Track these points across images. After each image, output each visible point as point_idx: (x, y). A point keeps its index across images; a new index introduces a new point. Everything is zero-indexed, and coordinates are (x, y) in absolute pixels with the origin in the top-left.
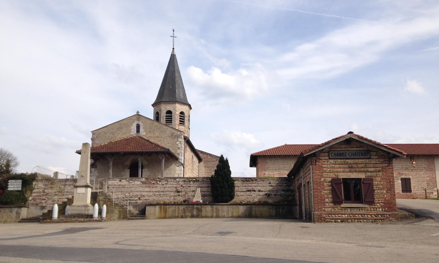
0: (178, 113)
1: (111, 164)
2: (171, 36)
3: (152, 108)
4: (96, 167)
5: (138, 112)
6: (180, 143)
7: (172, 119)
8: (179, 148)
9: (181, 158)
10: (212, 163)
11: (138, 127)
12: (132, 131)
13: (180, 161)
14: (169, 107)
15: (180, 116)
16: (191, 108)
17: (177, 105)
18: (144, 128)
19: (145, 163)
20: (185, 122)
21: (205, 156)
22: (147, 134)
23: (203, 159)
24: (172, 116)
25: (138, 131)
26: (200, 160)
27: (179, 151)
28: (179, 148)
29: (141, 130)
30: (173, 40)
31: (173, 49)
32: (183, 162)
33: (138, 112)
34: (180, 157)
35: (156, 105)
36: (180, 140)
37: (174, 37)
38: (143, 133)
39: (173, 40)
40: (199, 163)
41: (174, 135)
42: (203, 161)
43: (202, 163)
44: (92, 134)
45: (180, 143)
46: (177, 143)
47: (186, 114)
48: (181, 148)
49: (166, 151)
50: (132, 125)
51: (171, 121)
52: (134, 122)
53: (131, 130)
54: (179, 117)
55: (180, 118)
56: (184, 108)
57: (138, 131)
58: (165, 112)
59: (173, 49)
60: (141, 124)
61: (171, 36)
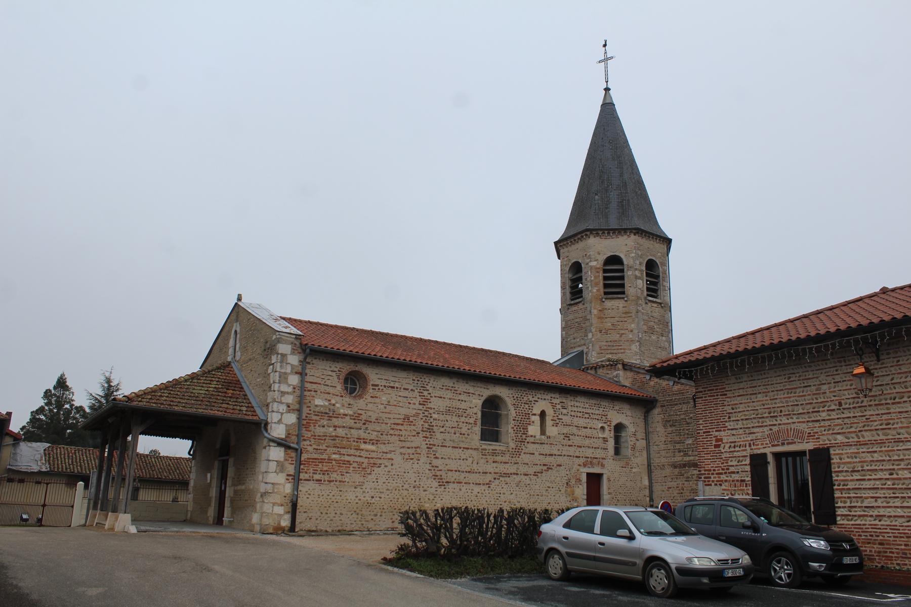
15: (605, 271)
16: (669, 241)
17: (592, 241)
42: (658, 404)
43: (656, 411)
54: (601, 275)
55: (605, 278)
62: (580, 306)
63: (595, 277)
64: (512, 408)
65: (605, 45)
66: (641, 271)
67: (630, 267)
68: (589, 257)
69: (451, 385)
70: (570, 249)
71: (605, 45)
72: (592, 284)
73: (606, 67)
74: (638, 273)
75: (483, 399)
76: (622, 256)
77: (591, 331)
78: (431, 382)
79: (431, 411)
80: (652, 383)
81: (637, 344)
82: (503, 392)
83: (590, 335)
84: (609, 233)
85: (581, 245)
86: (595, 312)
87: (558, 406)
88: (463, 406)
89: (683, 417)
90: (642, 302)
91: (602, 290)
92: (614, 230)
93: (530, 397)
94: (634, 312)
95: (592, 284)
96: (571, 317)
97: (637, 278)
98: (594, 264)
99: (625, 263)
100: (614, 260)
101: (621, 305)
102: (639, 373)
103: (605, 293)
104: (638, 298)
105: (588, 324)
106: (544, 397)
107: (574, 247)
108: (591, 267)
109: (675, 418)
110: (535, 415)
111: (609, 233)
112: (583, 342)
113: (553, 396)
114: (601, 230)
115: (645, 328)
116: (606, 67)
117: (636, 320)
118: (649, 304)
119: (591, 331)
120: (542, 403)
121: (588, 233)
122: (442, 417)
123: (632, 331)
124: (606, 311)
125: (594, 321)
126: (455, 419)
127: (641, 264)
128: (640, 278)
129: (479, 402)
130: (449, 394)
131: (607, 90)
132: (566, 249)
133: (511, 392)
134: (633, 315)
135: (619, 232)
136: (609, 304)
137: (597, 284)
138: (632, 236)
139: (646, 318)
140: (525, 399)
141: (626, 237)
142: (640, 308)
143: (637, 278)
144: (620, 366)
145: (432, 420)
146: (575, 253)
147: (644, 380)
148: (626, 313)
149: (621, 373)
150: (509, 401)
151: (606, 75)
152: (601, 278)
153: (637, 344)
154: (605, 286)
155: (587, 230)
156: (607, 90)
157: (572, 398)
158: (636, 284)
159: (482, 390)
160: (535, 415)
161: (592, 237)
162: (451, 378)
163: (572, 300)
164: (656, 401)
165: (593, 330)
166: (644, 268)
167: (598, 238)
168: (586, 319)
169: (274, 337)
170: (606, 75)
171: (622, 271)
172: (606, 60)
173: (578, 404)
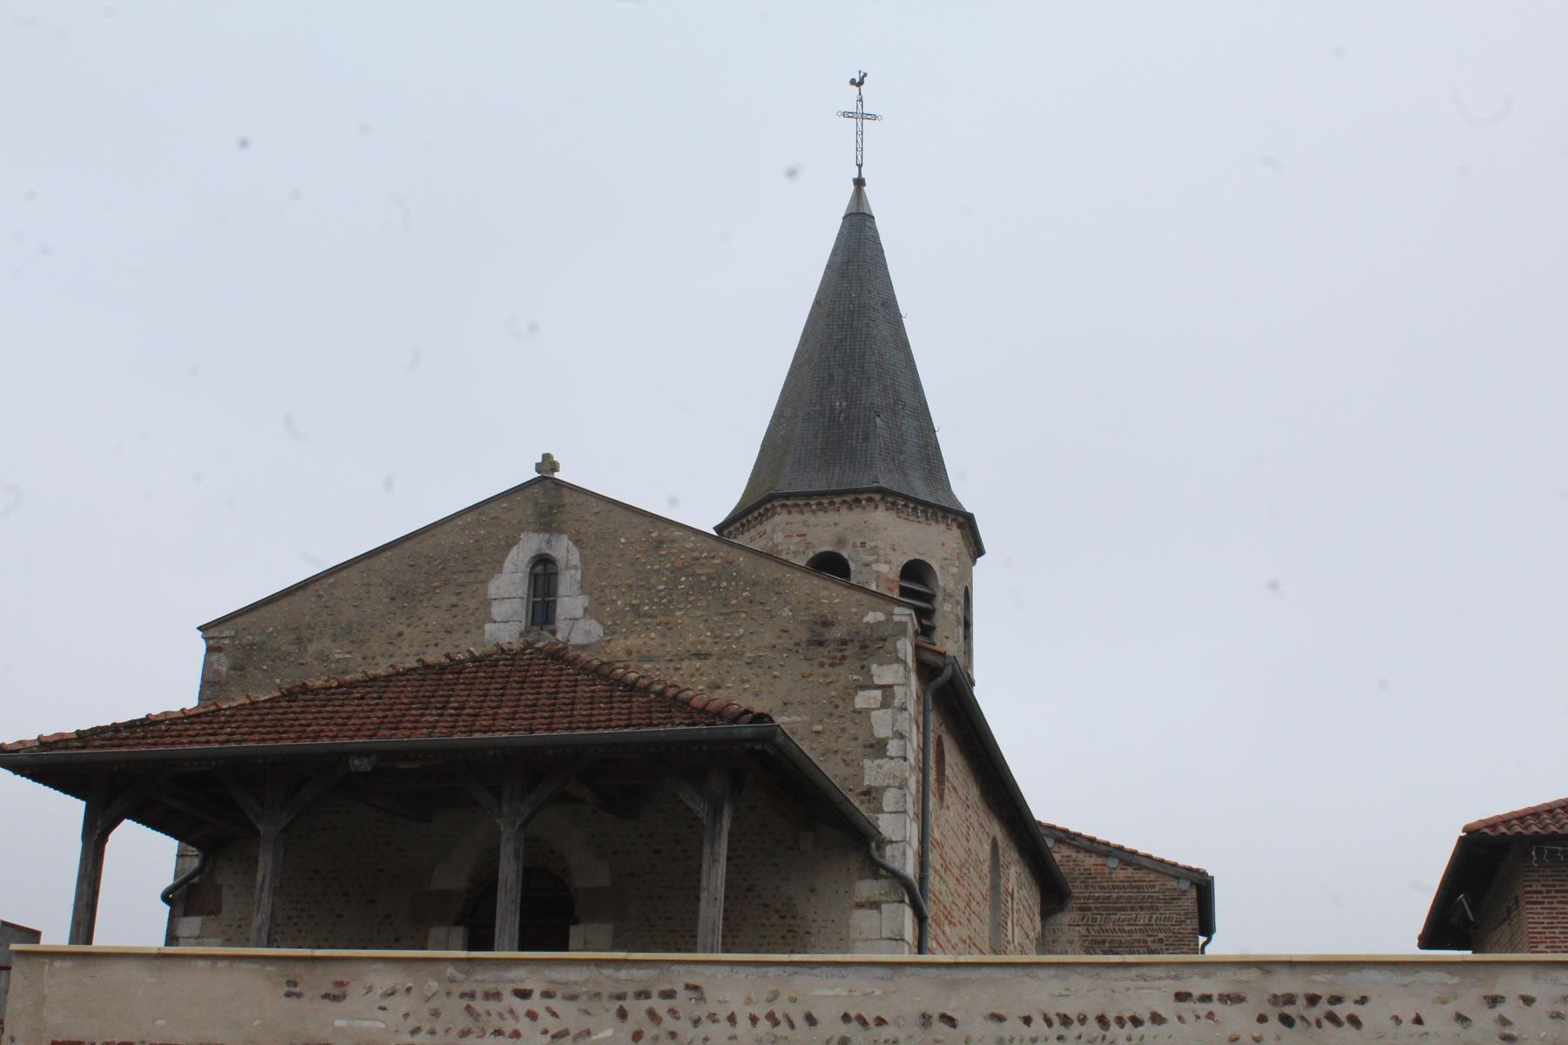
1: (265, 865)
2: (846, 114)
4: (213, 911)
5: (548, 464)
6: (886, 703)
8: (878, 748)
9: (897, 828)
10: (1143, 918)
11: (543, 573)
12: (498, 611)
13: (891, 857)
14: (823, 530)
16: (978, 550)
17: (881, 517)
18: (585, 588)
19: (588, 872)
21: (1090, 861)
22: (610, 631)
23: (1077, 890)
25: (542, 608)
26: (1053, 892)
27: (874, 772)
28: (878, 748)
29: (570, 602)
30: (860, 133)
32: (910, 870)
33: (548, 464)
34: (886, 825)
36: (885, 674)
37: (861, 116)
38: (577, 623)
39: (860, 133)
40: (1045, 915)
41: (837, 633)
42: (1072, 904)
43: (1066, 918)
44: (201, 647)
45: (886, 703)
46: (863, 699)
47: (944, 580)
48: (893, 747)
49: (746, 729)
50: (497, 566)
52: (512, 542)
53: (487, 603)
57: (542, 608)
60: (564, 550)
61: (846, 114)
67: (948, 596)
70: (807, 516)
76: (936, 567)
84: (914, 509)
89: (1137, 936)
98: (883, 568)
107: (832, 517)
109: (1117, 936)
121: (877, 497)
131: (859, 183)
132: (796, 517)
141: (943, 527)
155: (879, 490)
156: (859, 183)
161: (882, 507)
167: (892, 514)
169: (881, 617)
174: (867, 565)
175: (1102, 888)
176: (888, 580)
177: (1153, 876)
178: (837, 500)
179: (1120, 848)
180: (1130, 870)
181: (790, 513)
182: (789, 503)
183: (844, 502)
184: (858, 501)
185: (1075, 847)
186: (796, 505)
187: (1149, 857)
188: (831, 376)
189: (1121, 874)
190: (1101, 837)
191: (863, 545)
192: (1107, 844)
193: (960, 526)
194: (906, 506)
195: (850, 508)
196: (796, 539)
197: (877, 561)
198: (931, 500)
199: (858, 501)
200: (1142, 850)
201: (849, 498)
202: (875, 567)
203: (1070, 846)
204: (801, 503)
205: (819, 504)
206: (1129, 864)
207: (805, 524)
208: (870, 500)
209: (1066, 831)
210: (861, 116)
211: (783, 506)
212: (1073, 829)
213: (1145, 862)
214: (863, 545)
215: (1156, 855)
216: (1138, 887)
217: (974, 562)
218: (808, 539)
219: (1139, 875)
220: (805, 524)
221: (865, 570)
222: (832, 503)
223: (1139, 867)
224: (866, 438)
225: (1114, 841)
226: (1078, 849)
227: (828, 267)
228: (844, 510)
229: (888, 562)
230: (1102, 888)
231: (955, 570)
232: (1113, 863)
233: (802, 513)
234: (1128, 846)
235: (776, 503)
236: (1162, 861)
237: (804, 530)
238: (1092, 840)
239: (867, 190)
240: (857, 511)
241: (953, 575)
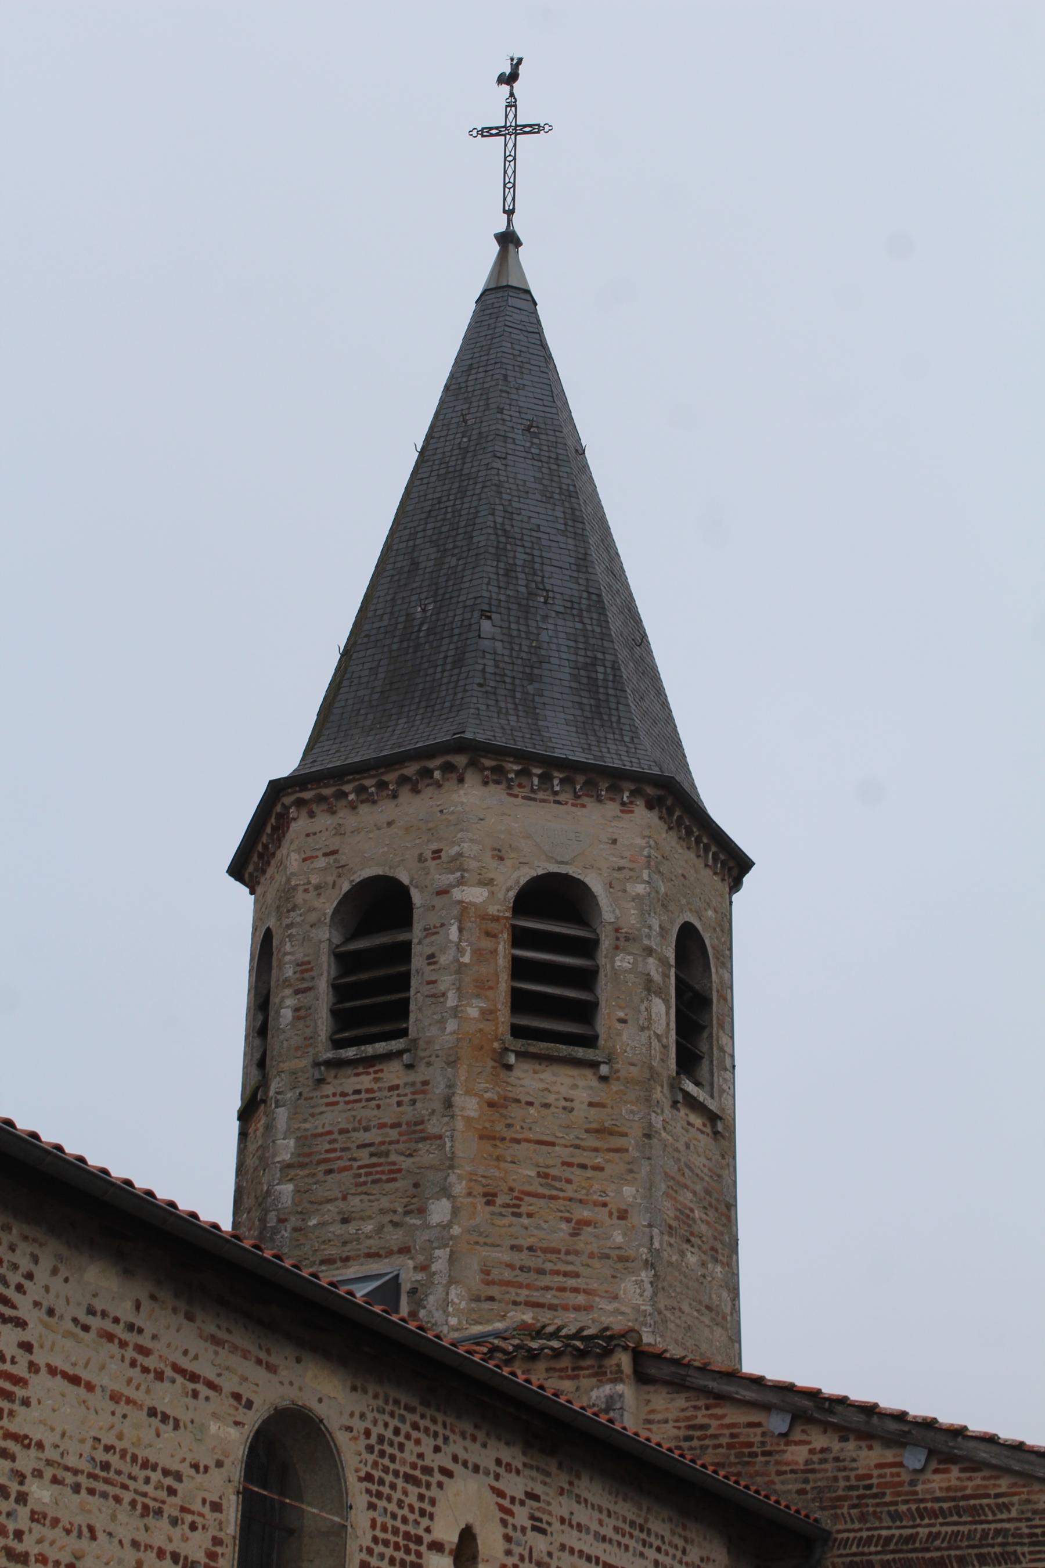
0: (490, 895)
3: (240, 902)
7: (403, 982)
15: (520, 938)
16: (734, 865)
17: (472, 797)
20: (605, 1022)
21: (868, 1458)
24: (404, 952)
31: (508, 240)
35: (266, 857)
51: (402, 1010)
54: (503, 950)
55: (519, 969)
56: (599, 843)
58: (328, 905)
59: (508, 240)
62: (393, 1073)
63: (479, 954)
64: (357, 1494)
65: (509, 79)
66: (663, 961)
67: (624, 939)
68: (457, 863)
69: (125, 1310)
70: (347, 819)
71: (509, 79)
72: (462, 981)
73: (510, 159)
74: (652, 965)
75: (253, 1419)
76: (596, 884)
77: (445, 1192)
78: (42, 1273)
79: (26, 1460)
80: (797, 1454)
81: (645, 1276)
82: (327, 1394)
83: (439, 1211)
84: (546, 778)
85: (412, 807)
86: (468, 1106)
87: (521, 1516)
88: (167, 1448)
90: (661, 1094)
91: (504, 1016)
92: (570, 767)
93: (427, 1445)
94: (636, 1131)
95: (462, 981)
96: (333, 1118)
97: (649, 987)
98: (475, 895)
99: (607, 911)
100: (554, 903)
101: (582, 1096)
102: (721, 1398)
103: (517, 1031)
104: (653, 1075)
105: (427, 1154)
106: (476, 1454)
108: (464, 908)
110: (437, 1547)
111: (546, 778)
112: (394, 1238)
113: (507, 1454)
114: (519, 755)
115: (667, 1207)
116: (510, 159)
117: (645, 1169)
118: (683, 1111)
119: (445, 1192)
120: (470, 1492)
121: (460, 760)
122: (71, 1507)
123: (623, 1215)
124: (515, 1112)
125: (465, 1146)
126: (128, 1525)
127: (663, 931)
128: (660, 992)
129: (230, 1438)
130: (110, 1369)
132: (324, 821)
133: (360, 1403)
134: (629, 1143)
135: (590, 785)
136: (530, 1080)
137: (483, 987)
138: (640, 809)
139: (672, 1167)
140: (410, 1454)
141: (612, 808)
142: (657, 1121)
143: (649, 987)
144: (624, 1360)
145: (23, 1512)
146: (374, 839)
147: (754, 1436)
148: (600, 1131)
149: (625, 1389)
150: (352, 1456)
151: (509, 185)
152: (503, 962)
153: (645, 1276)
154: (520, 1001)
155: (461, 746)
157: (562, 1479)
158: (637, 1021)
159: (248, 1368)
160: (437, 1547)
161: (472, 778)
162: (127, 1273)
163: (338, 1044)
164: (825, 1537)
165: (459, 1188)
166: (671, 954)
168: (416, 1133)
170: (509, 185)
171: (588, 947)
172: (512, 130)
173: (582, 1515)
174: (443, 892)
175: (895, 1516)
176: (485, 917)
177: (1004, 1484)
178: (391, 777)
179: (929, 1425)
180: (955, 1471)
181: (312, 815)
182: (307, 795)
183: (403, 780)
184: (427, 773)
185: (837, 1428)
186: (321, 799)
187: (991, 1440)
188: (415, 564)
189: (936, 1483)
190: (889, 1401)
191: (437, 854)
192: (901, 1417)
193: (650, 806)
194: (525, 773)
195: (416, 791)
196: (321, 862)
197: (461, 882)
198: (580, 757)
199: (427, 773)
200: (976, 1426)
201: (411, 770)
202: (457, 894)
203: (826, 1427)
204: (327, 792)
205: (361, 790)
206: (951, 1459)
207: (339, 831)
208: (448, 768)
209: (814, 1395)
210: (512, 130)
211: (300, 803)
212: (830, 1389)
213: (984, 1453)
214: (437, 854)
215: (1007, 1433)
216: (974, 1511)
217: (736, 885)
218: (343, 859)
219: (977, 1480)
220: (339, 831)
221: (438, 902)
222: (382, 785)
223: (974, 1466)
224: (459, 662)
225: (917, 1408)
226: (844, 1432)
227: (447, 388)
228: (405, 794)
229: (487, 883)
230: (895, 1516)
231: (641, 889)
232: (914, 1459)
233: (333, 812)
234: (947, 1417)
235: (287, 800)
236: (1019, 1447)
237: (335, 843)
238: (870, 1410)
239: (525, 255)
240: (428, 792)
241: (637, 898)
